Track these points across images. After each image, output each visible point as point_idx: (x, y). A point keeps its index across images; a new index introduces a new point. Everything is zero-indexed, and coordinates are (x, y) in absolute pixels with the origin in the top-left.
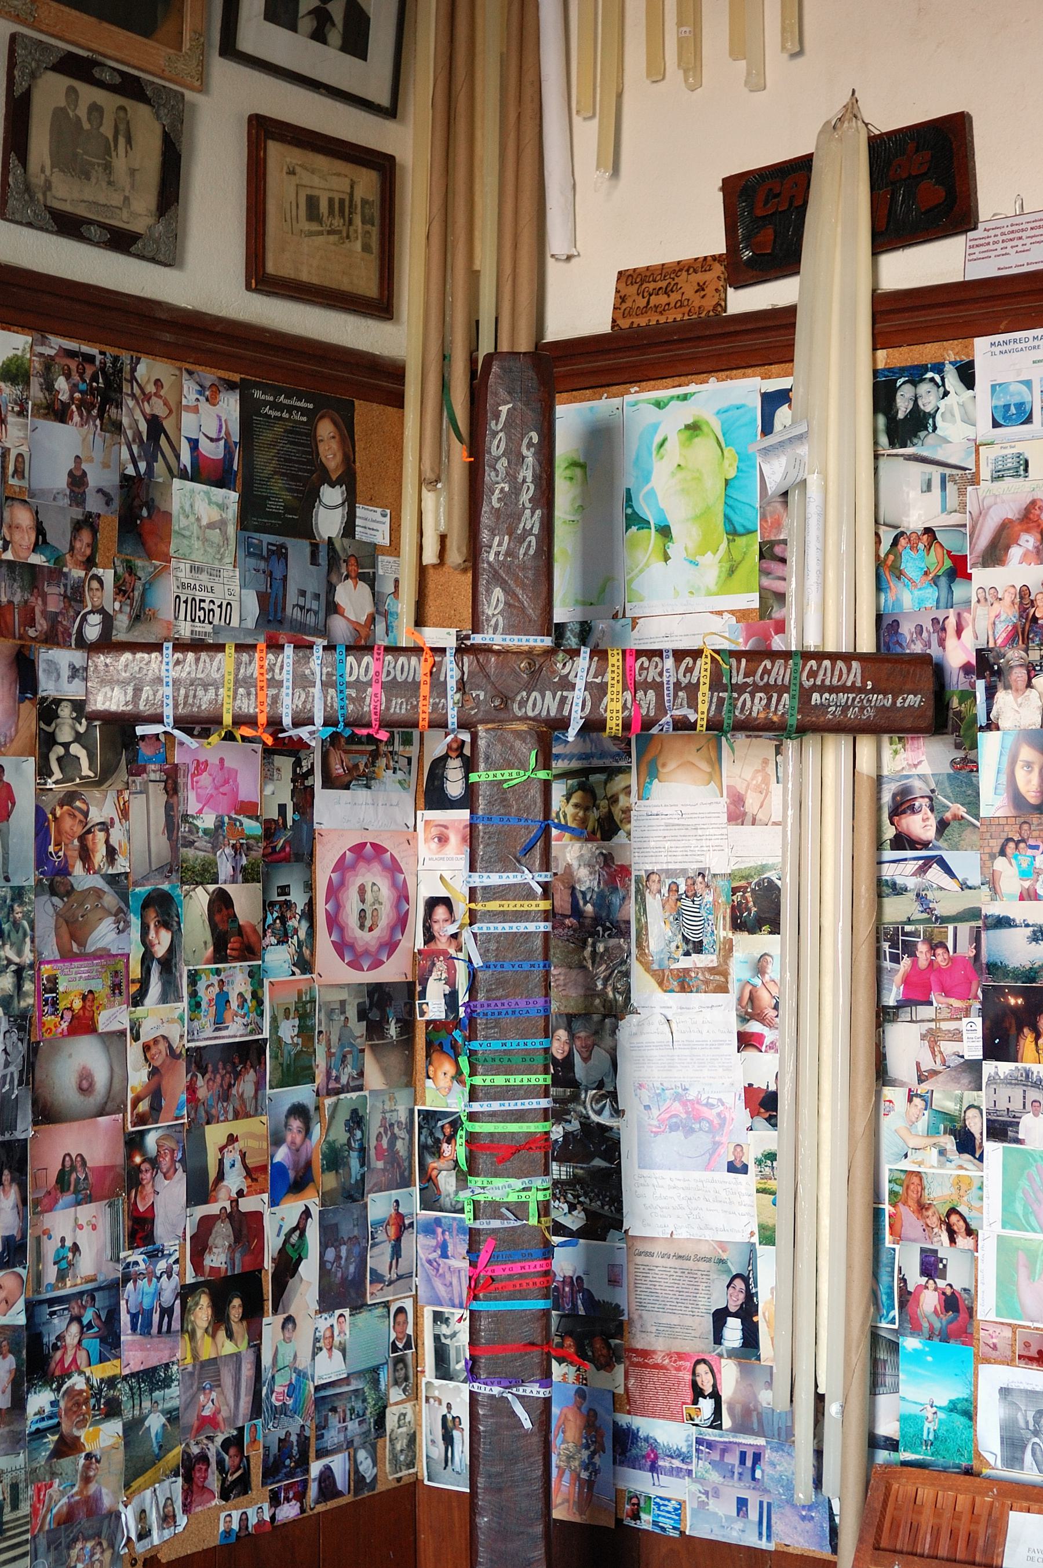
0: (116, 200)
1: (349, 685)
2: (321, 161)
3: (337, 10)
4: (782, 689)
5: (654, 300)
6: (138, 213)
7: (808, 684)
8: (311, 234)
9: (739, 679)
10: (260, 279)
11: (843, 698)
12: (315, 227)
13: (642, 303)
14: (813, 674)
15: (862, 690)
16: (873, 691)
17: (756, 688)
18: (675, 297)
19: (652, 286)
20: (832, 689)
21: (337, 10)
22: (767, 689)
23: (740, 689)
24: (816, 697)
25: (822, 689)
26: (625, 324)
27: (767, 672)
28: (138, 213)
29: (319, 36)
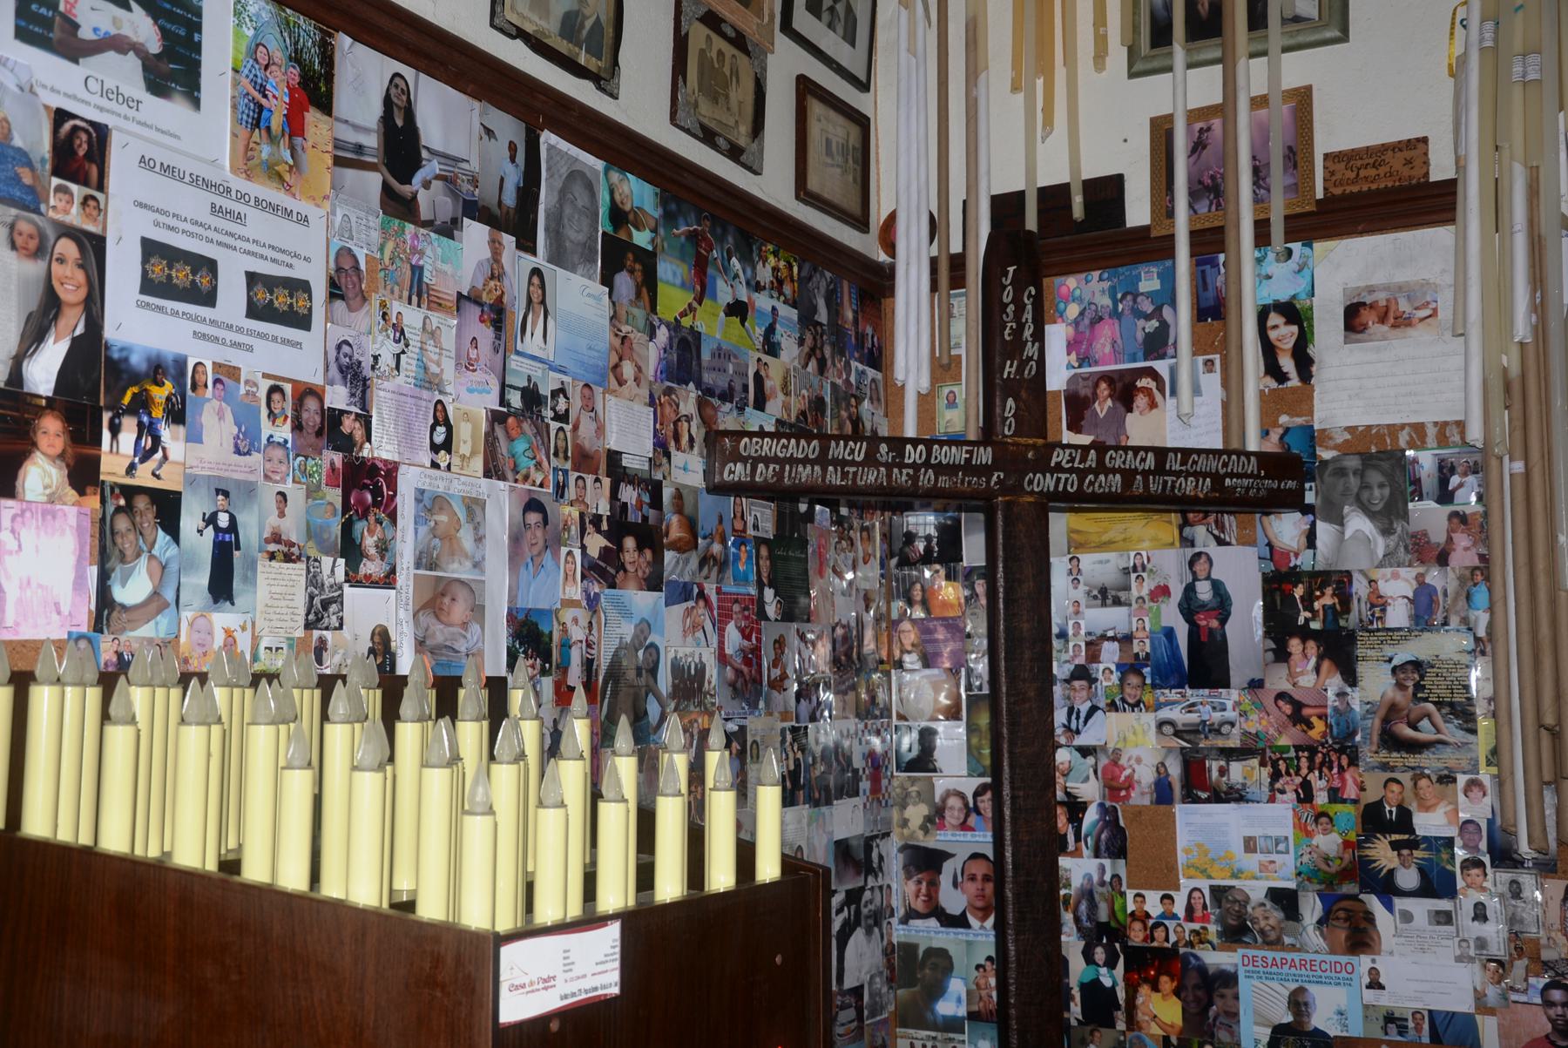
0: (731, 122)
1: (908, 466)
2: (832, 114)
3: (840, 8)
4: (1205, 475)
5: (1363, 173)
6: (742, 136)
7: (1222, 471)
8: (826, 165)
9: (1177, 467)
10: (803, 192)
11: (1246, 482)
12: (829, 161)
13: (1353, 175)
14: (1225, 465)
15: (1258, 476)
16: (1266, 477)
17: (1188, 474)
18: (1382, 170)
19: (1359, 163)
20: (1239, 476)
21: (840, 8)
22: (1196, 474)
23: (1178, 474)
24: (1228, 481)
25: (1232, 475)
26: (1338, 191)
27: (1195, 462)
28: (742, 136)
29: (830, 26)
